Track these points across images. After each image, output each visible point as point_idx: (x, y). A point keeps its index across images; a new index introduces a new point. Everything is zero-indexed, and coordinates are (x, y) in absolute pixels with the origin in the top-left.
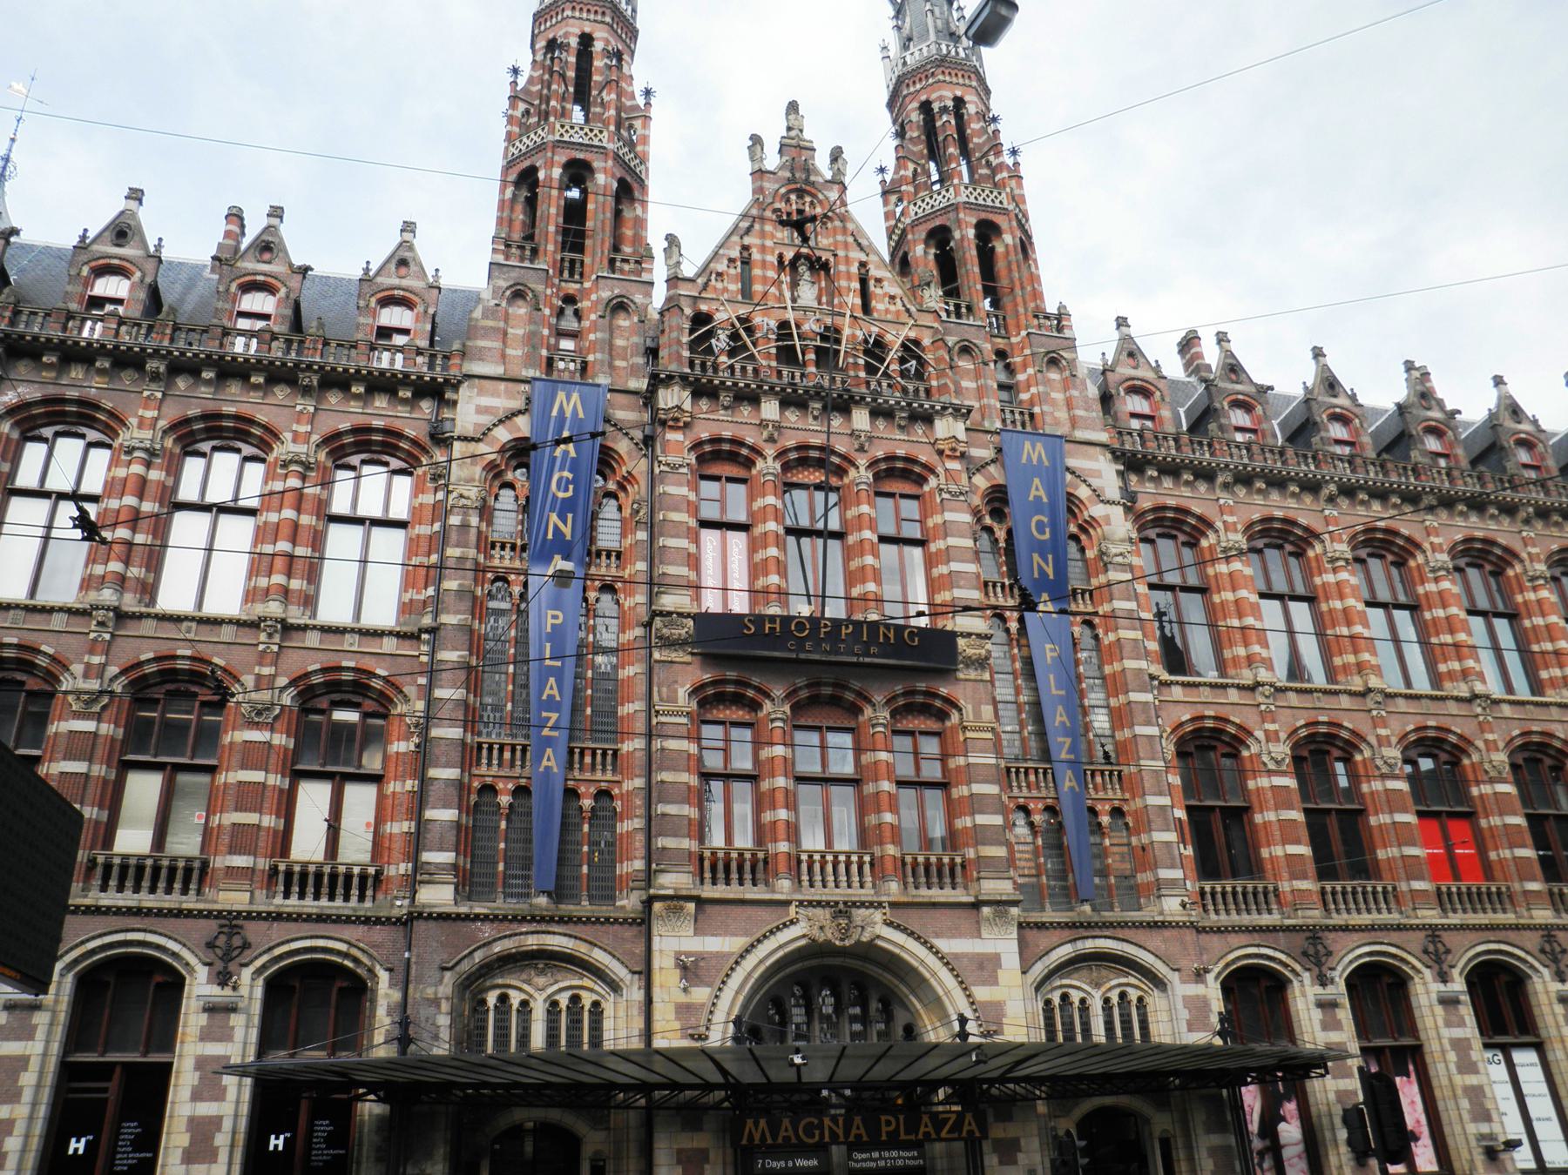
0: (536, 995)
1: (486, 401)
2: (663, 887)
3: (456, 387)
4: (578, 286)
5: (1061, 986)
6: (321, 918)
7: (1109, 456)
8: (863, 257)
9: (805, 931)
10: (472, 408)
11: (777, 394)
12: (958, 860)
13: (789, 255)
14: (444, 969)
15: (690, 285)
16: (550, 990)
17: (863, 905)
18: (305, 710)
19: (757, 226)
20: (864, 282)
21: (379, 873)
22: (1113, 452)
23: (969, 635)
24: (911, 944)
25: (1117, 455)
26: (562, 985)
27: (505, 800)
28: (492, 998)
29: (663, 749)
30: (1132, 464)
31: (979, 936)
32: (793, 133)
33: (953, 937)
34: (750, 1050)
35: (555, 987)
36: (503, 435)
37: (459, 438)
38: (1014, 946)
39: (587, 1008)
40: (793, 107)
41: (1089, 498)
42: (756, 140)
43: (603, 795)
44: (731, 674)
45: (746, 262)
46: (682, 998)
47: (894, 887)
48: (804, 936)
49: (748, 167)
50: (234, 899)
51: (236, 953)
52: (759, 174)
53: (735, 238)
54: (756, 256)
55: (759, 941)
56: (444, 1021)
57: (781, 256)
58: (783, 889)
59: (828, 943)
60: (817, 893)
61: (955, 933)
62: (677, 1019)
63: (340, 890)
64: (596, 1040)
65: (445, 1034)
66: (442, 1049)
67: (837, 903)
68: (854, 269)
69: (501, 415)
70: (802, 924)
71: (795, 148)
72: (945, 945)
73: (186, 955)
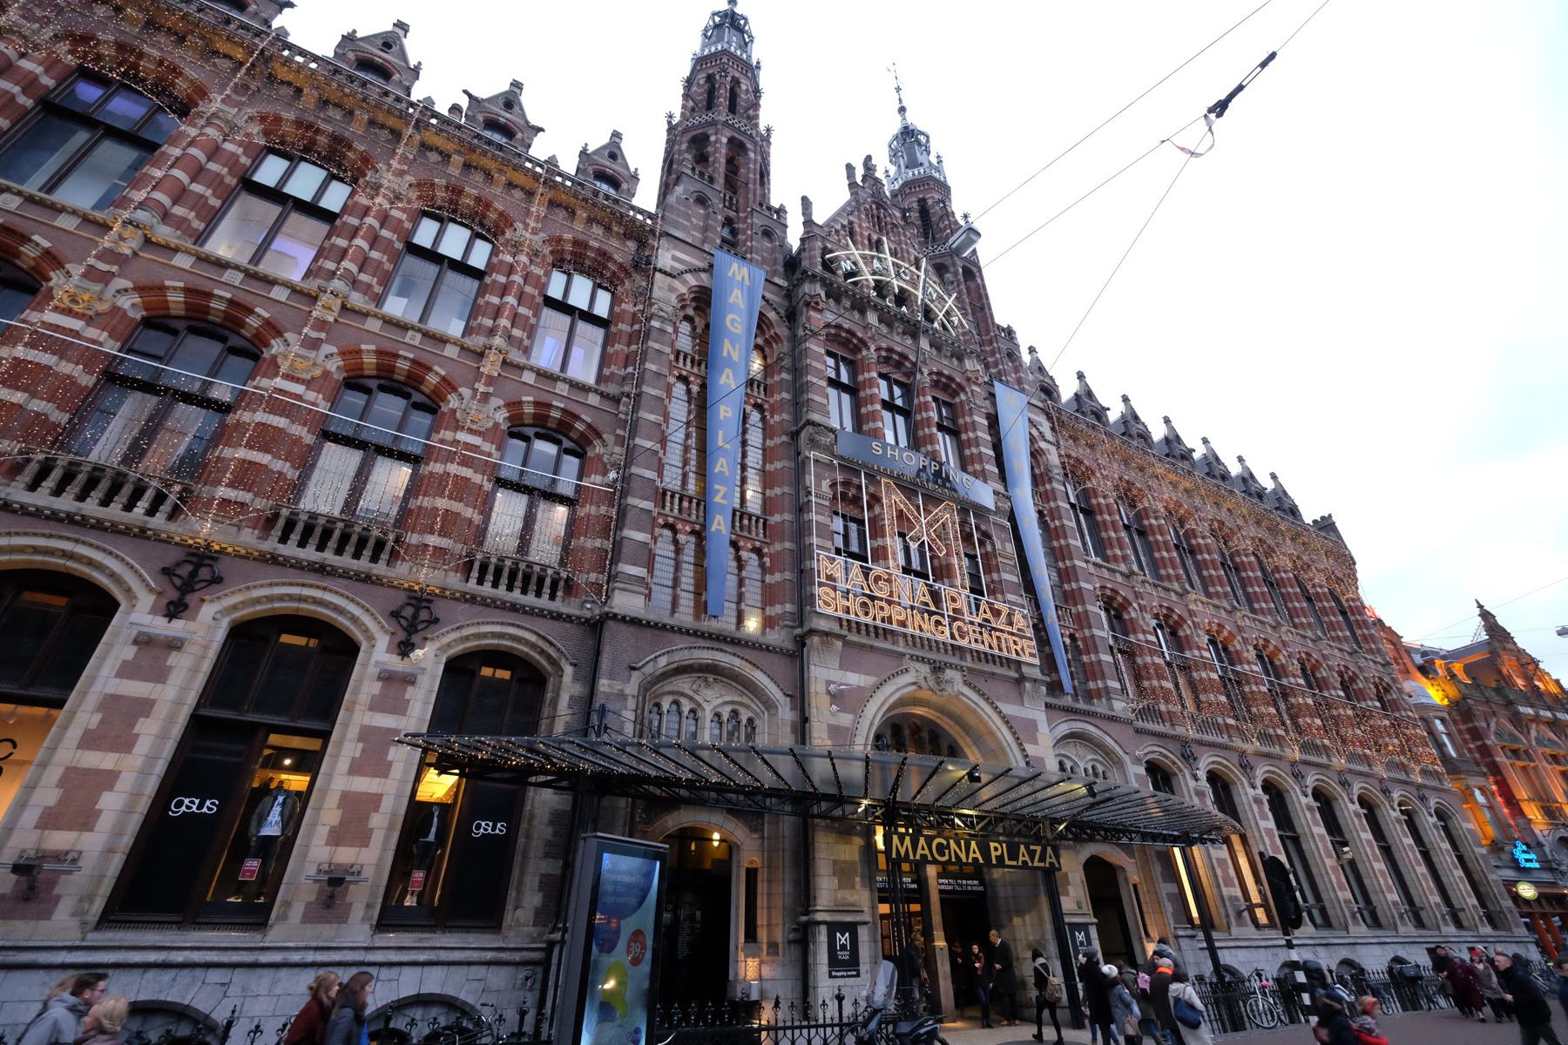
0: (705, 705)
9: (914, 680)
14: (634, 669)
17: (951, 666)
31: (1023, 705)
36: (691, 280)
46: (833, 721)
48: (914, 684)
50: (426, 576)
51: (421, 627)
62: (830, 738)
63: (533, 587)
73: (366, 619)
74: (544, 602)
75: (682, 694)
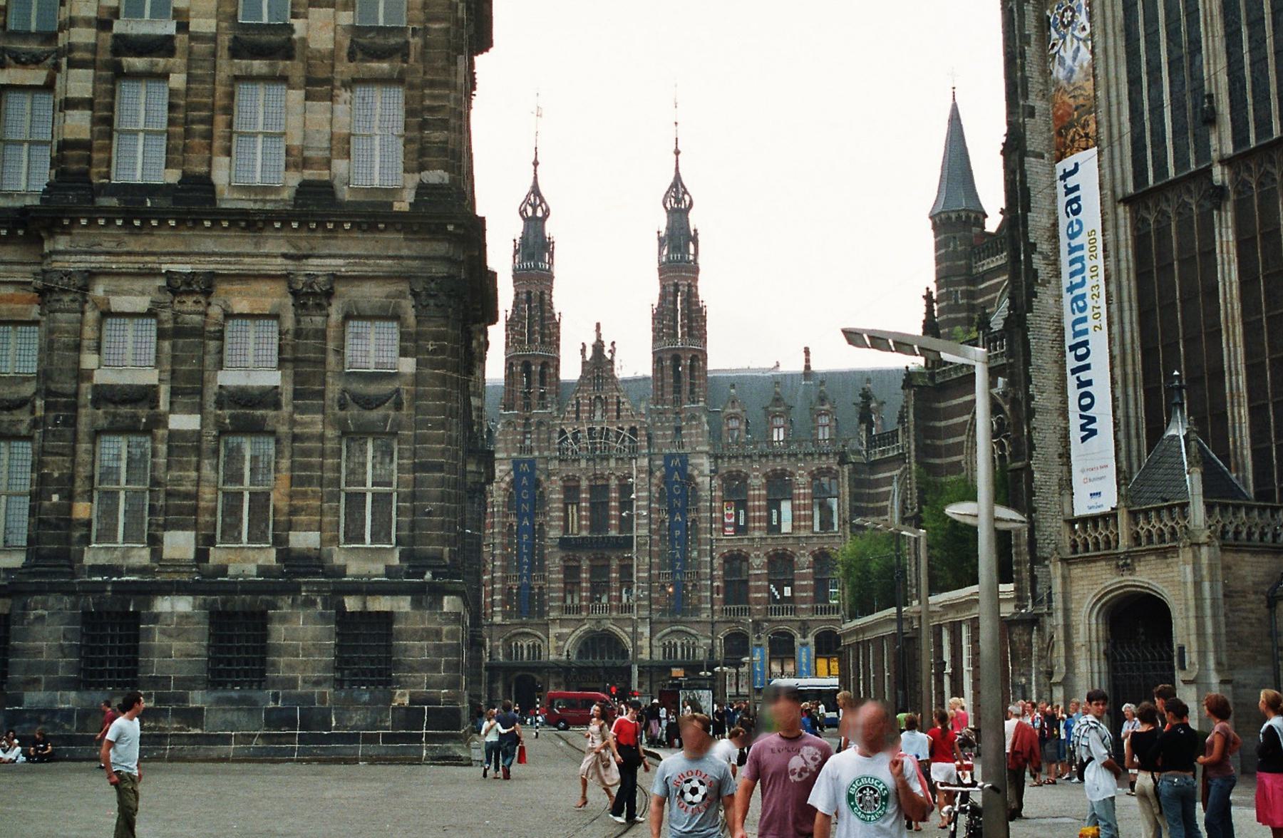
1: (502, 467)
8: (617, 394)
13: (593, 397)
24: (619, 630)
25: (710, 456)
30: (715, 457)
36: (507, 479)
38: (648, 630)
40: (598, 325)
43: (541, 588)
45: (578, 403)
47: (614, 614)
52: (584, 363)
58: (584, 614)
71: (598, 347)
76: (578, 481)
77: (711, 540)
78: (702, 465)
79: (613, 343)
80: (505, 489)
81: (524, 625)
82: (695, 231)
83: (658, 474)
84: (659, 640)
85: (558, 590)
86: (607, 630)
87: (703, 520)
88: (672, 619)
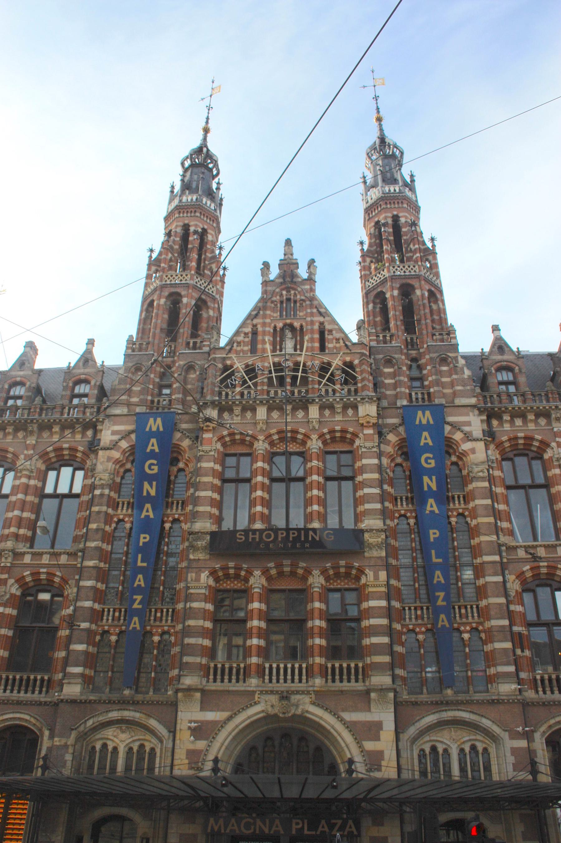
0: (120, 744)
2: (183, 684)
3: (103, 422)
4: (171, 359)
5: (431, 741)
6: (19, 703)
7: (476, 412)
8: (321, 319)
9: (263, 708)
10: (110, 432)
11: (265, 404)
12: (360, 665)
13: (280, 325)
14: (73, 729)
15: (222, 351)
16: (127, 742)
17: (297, 692)
18: (24, 595)
19: (261, 312)
20: (322, 333)
21: (49, 680)
22: (479, 409)
23: (371, 530)
25: (481, 411)
26: (135, 738)
27: (114, 638)
28: (98, 746)
29: (190, 608)
32: (286, 257)
33: (354, 711)
34: (251, 778)
35: (131, 740)
36: (124, 444)
37: (101, 449)
38: (391, 717)
39: (147, 751)
41: (461, 439)
42: (266, 266)
44: (231, 564)
45: (255, 333)
46: (191, 747)
48: (263, 711)
49: (260, 280)
52: (265, 283)
53: (249, 321)
54: (260, 329)
55: (235, 714)
56: (68, 757)
57: (275, 327)
59: (276, 715)
60: (270, 687)
61: (356, 709)
62: (187, 758)
64: (151, 769)
65: (69, 764)
66: (67, 772)
67: (282, 692)
68: (316, 327)
69: (124, 435)
70: (262, 704)
72: (348, 716)
74: (36, 696)
75: (108, 739)
76: (251, 445)
77: (500, 545)
78: (469, 424)
79: (312, 262)
80: (117, 462)
81: (124, 703)
82: (412, 176)
83: (392, 438)
84: (414, 740)
85: (203, 633)
86: (303, 719)
87: (480, 511)
88: (436, 697)
